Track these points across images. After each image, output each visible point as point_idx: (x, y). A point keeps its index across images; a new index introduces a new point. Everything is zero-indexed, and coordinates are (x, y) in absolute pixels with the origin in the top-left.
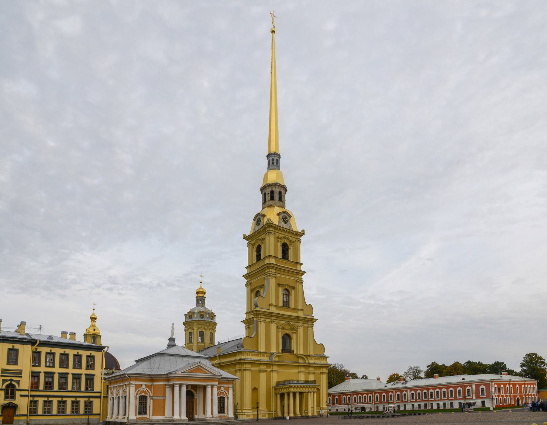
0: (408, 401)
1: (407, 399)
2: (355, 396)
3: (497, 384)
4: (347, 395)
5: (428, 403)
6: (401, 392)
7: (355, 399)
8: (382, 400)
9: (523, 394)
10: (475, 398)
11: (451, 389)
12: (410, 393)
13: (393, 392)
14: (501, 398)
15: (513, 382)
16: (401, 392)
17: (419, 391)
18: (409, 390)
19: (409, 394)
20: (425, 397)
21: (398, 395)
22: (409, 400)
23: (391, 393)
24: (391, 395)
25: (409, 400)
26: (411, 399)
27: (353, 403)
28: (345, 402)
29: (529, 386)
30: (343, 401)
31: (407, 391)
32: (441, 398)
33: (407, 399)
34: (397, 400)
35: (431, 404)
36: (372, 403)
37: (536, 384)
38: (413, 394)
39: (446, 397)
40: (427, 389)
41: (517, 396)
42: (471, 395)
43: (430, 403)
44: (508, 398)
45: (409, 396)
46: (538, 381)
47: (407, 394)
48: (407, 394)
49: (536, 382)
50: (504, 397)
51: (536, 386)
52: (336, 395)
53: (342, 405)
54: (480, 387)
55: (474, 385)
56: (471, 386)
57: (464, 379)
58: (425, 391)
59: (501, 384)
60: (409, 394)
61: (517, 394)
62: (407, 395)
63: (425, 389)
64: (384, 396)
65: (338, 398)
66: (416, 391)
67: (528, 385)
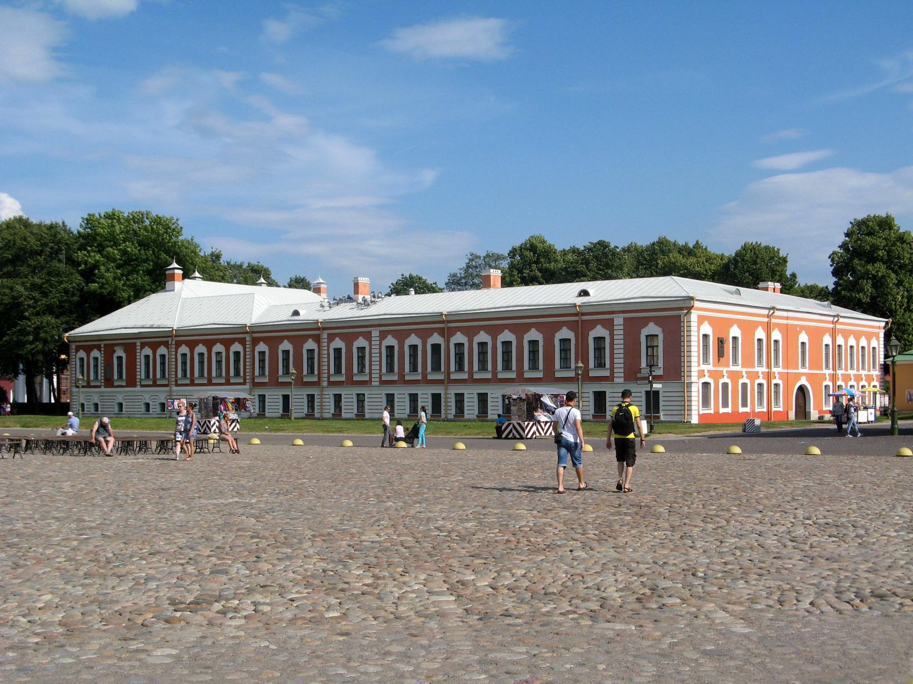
0: (371, 378)
1: (371, 369)
2: (184, 349)
3: (712, 321)
4: (154, 346)
5: (446, 389)
6: (349, 339)
7: (184, 363)
8: (280, 372)
9: (824, 371)
10: (622, 380)
11: (533, 334)
12: (380, 345)
13: (317, 339)
14: (729, 381)
15: (787, 318)
16: (349, 339)
17: (414, 340)
18: (375, 333)
19: (375, 351)
20: (436, 367)
21: (338, 351)
22: (375, 376)
23: (310, 344)
24: (311, 352)
25: (375, 376)
26: (384, 370)
27: (176, 381)
28: (148, 376)
29: (852, 341)
30: (141, 373)
31: (368, 336)
32: (495, 372)
33: (371, 369)
34: (332, 372)
35: (456, 395)
36: (244, 383)
37: (882, 335)
38: (390, 349)
39: (514, 368)
40: (441, 332)
41: (799, 379)
42: (608, 365)
43: (454, 390)
44: (760, 385)
45: (376, 359)
46: (887, 323)
47: (371, 349)
48: (371, 349)
49: (879, 328)
50: (741, 381)
51: (878, 343)
52: (118, 345)
53: (138, 388)
54: (645, 332)
55: (619, 320)
56: (609, 325)
57: (585, 293)
58: (436, 339)
59: (731, 322)
60: (375, 351)
61: (801, 370)
62: (370, 353)
63: (435, 330)
64: (286, 353)
65: (124, 355)
66: (401, 336)
67: (846, 334)
